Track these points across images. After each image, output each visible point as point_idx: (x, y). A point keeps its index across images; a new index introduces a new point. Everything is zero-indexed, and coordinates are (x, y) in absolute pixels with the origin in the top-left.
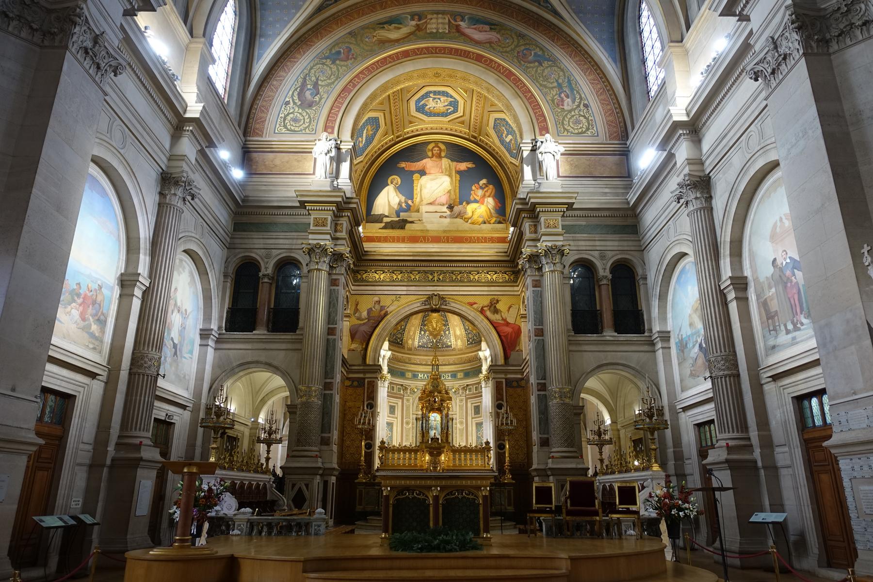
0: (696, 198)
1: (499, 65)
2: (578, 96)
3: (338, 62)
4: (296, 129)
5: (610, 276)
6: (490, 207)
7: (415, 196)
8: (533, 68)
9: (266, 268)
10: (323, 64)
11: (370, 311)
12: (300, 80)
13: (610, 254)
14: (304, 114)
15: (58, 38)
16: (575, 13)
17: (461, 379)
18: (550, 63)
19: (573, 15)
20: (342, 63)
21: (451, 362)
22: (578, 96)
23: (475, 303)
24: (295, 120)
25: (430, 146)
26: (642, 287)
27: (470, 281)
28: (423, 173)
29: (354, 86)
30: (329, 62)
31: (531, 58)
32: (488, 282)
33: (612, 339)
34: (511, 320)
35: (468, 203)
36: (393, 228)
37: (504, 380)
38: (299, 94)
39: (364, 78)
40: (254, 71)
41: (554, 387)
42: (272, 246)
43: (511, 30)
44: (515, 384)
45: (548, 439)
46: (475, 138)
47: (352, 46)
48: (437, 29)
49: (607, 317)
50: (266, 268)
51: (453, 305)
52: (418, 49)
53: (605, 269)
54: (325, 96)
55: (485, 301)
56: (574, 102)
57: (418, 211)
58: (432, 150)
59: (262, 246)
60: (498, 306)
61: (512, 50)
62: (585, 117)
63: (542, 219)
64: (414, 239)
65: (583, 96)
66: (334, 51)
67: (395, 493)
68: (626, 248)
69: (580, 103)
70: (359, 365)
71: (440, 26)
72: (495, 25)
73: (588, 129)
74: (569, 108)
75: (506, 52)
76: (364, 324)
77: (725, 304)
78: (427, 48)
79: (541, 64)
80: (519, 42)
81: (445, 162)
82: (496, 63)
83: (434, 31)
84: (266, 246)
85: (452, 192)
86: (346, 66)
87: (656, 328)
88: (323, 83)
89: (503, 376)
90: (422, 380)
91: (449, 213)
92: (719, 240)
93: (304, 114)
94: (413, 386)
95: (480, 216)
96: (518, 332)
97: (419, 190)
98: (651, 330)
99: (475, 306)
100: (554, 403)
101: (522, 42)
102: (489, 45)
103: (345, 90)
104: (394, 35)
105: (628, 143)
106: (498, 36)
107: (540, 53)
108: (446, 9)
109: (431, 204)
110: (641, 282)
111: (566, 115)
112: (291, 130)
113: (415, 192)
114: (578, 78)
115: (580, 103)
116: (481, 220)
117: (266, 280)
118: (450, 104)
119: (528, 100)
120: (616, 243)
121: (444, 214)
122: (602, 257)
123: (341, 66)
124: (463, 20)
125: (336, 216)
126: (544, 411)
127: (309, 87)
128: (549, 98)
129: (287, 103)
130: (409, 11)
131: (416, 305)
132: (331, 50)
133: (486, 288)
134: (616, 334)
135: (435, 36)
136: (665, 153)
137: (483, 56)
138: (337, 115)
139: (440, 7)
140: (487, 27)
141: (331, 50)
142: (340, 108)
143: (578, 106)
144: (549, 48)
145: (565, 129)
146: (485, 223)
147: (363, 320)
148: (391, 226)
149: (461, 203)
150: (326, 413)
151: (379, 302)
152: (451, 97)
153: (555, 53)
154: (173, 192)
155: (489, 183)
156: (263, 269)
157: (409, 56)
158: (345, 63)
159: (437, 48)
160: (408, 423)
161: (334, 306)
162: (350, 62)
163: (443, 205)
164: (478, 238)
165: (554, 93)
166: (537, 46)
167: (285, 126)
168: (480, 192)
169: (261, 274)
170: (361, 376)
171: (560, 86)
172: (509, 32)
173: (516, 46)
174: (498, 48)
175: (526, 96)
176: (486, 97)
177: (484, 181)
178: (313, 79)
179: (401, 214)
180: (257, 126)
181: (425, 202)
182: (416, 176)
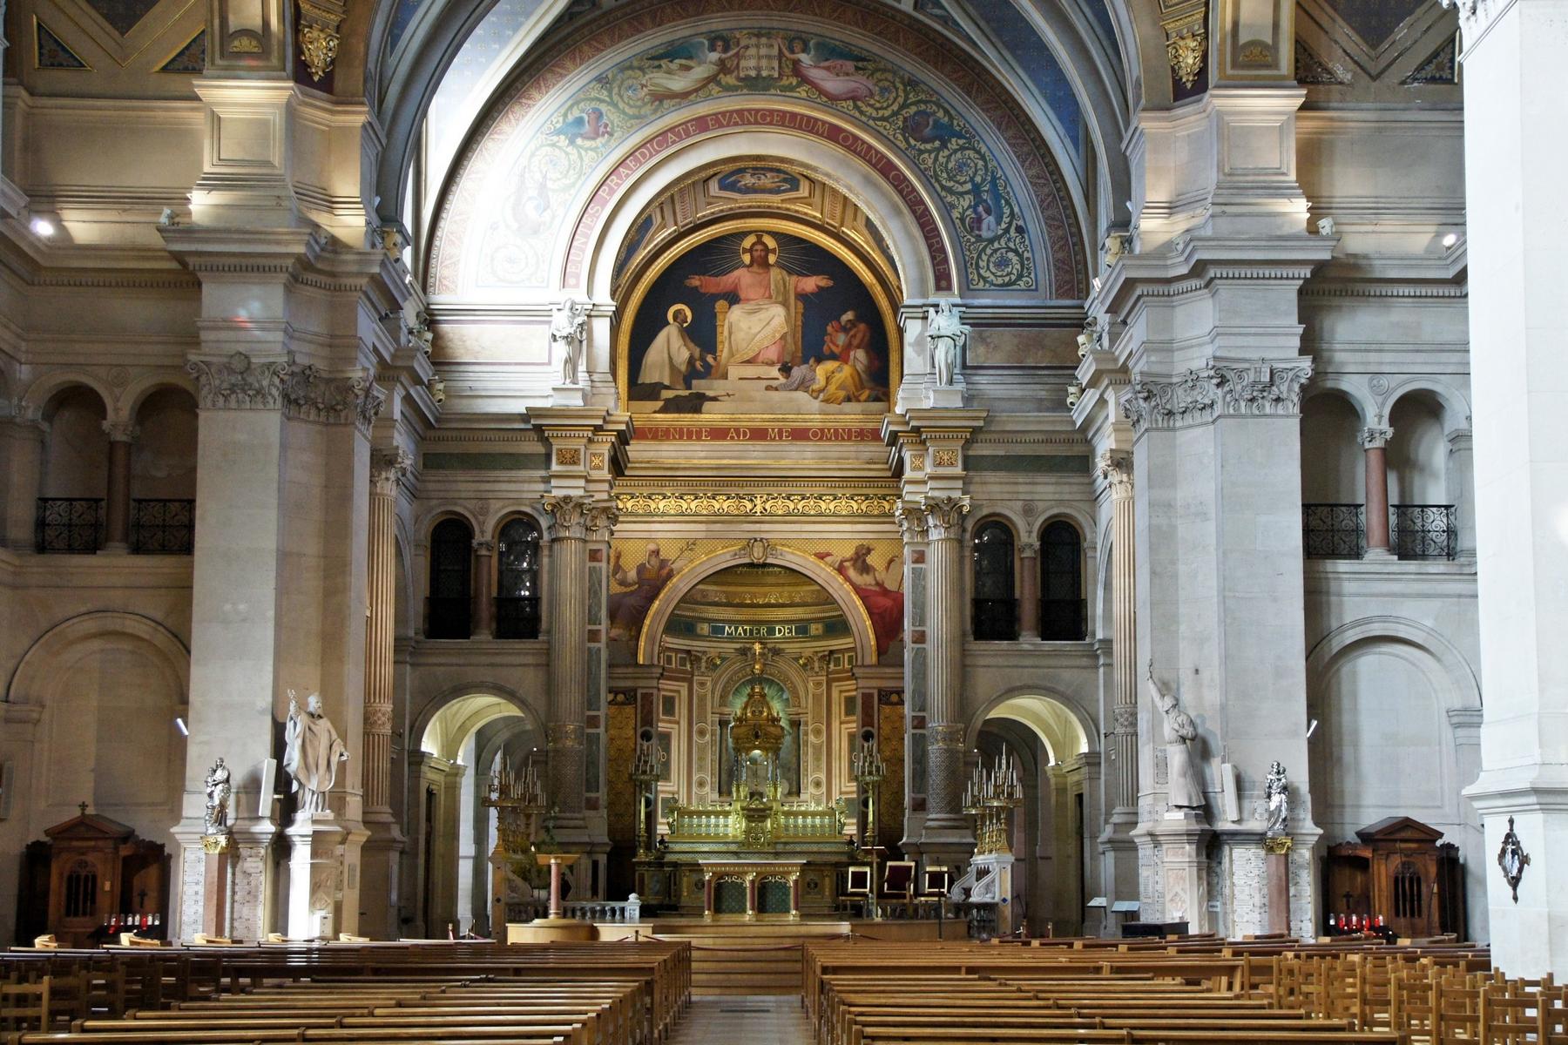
1: (870, 147)
2: (1007, 211)
3: (579, 141)
5: (1037, 544)
6: (860, 367)
7: (719, 347)
8: (930, 152)
9: (482, 532)
10: (553, 145)
11: (641, 569)
15: (343, 414)
16: (1007, 47)
17: (817, 638)
18: (961, 142)
19: (1005, 52)
20: (588, 143)
22: (1007, 211)
23: (828, 554)
25: (748, 242)
26: (1089, 561)
28: (733, 298)
30: (563, 141)
31: (927, 131)
32: (852, 515)
34: (891, 585)
35: (819, 361)
36: (679, 410)
41: (937, 724)
44: (894, 698)
45: (924, 800)
47: (603, 108)
48: (758, 69)
49: (1028, 610)
51: (789, 557)
53: (1030, 532)
55: (849, 552)
56: (999, 223)
57: (725, 376)
58: (751, 250)
59: (472, 495)
60: (869, 560)
61: (895, 114)
62: (1016, 251)
63: (931, 450)
64: (719, 434)
65: (1016, 209)
66: (570, 118)
69: (1010, 224)
70: (626, 666)
71: (764, 63)
72: (863, 59)
73: (1020, 277)
75: (883, 119)
76: (632, 593)
78: (740, 112)
79: (944, 146)
80: (907, 98)
81: (776, 274)
82: (864, 142)
83: (753, 73)
84: (479, 495)
86: (594, 149)
87: (1100, 635)
89: (875, 683)
90: (731, 638)
91: (782, 380)
94: (713, 653)
95: (841, 387)
97: (726, 333)
98: (1094, 635)
99: (828, 559)
100: (935, 750)
104: (678, 83)
108: (775, 24)
109: (749, 362)
110: (1089, 554)
111: (984, 249)
113: (719, 338)
114: (1009, 173)
115: (1010, 224)
116: (842, 394)
120: (1051, 489)
121: (774, 383)
122: (1028, 511)
123: (586, 150)
124: (805, 50)
125: (590, 440)
126: (920, 759)
128: (956, 214)
130: (704, 29)
132: (565, 115)
134: (1038, 641)
135: (755, 84)
139: (760, 20)
140: (849, 65)
141: (565, 115)
143: (1007, 231)
145: (980, 275)
146: (849, 399)
147: (630, 585)
148: (672, 406)
149: (806, 361)
150: (592, 763)
151: (657, 553)
154: (384, 475)
155: (859, 318)
159: (757, 111)
160: (702, 733)
161: (596, 593)
162: (600, 141)
163: (772, 364)
164: (836, 431)
166: (939, 106)
168: (841, 339)
169: (475, 543)
170: (629, 684)
171: (976, 190)
172: (890, 76)
174: (870, 110)
176: (845, 198)
177: (849, 316)
178: (538, 176)
182: (720, 305)
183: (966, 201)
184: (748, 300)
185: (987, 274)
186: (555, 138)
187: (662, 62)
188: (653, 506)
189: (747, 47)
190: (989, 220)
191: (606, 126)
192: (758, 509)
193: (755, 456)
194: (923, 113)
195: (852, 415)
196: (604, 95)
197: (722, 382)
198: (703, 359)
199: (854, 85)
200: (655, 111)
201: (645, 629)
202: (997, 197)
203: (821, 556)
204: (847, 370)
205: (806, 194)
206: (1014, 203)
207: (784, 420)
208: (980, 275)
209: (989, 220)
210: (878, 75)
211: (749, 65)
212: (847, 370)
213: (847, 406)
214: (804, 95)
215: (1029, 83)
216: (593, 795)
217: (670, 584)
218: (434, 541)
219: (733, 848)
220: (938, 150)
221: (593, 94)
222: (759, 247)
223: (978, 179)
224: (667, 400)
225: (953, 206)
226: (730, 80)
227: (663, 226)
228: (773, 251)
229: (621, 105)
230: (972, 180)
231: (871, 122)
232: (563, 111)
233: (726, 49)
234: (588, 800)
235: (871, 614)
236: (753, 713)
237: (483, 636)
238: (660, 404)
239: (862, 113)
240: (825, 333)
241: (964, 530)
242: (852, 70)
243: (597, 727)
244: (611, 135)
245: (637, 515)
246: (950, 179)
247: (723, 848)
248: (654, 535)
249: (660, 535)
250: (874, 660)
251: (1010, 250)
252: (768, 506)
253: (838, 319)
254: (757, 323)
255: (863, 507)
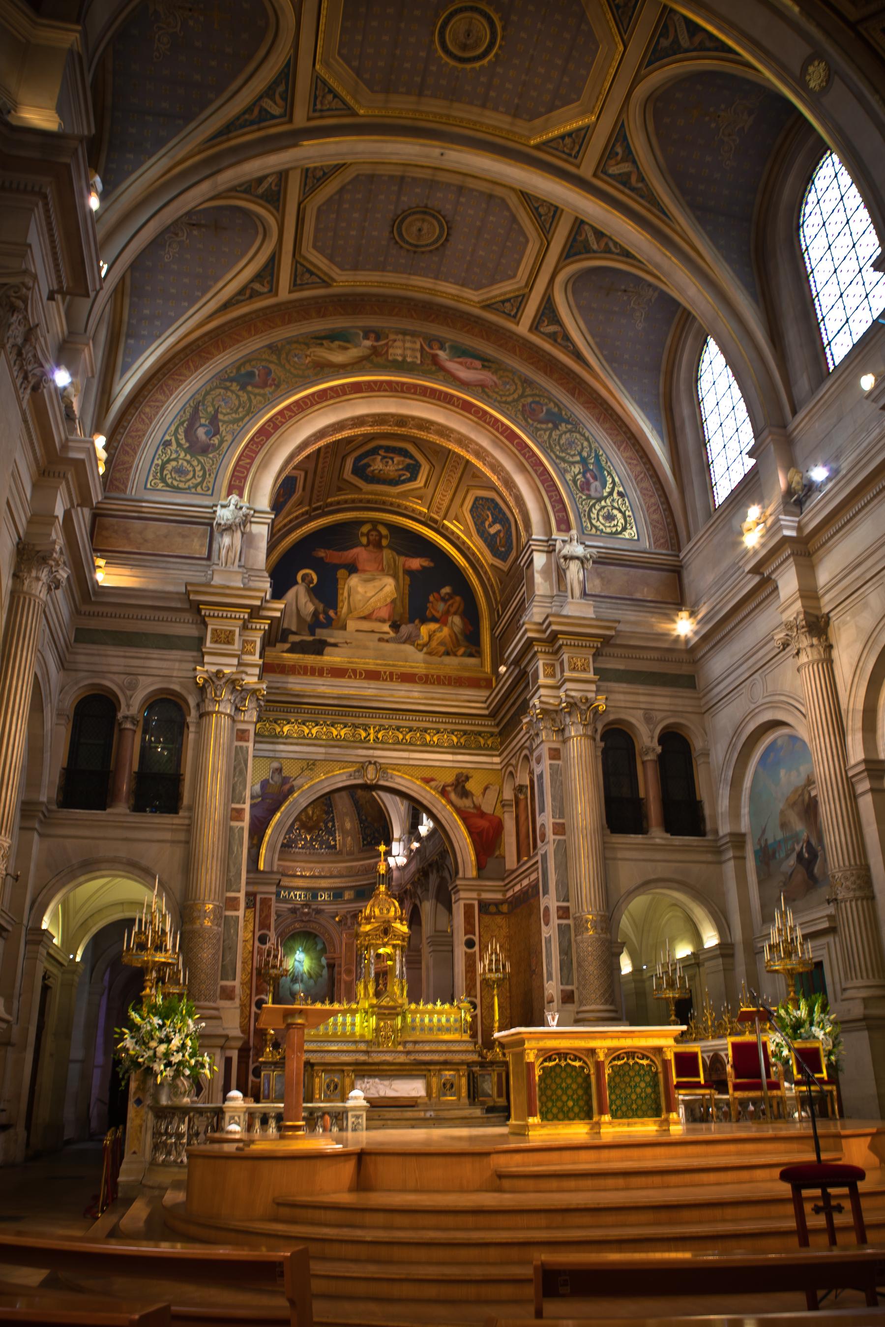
0: (812, 646)
2: (609, 480)
3: (249, 388)
4: (181, 485)
5: (659, 749)
6: (456, 629)
7: (340, 605)
8: (545, 430)
9: (128, 706)
10: (227, 389)
12: (189, 410)
13: (660, 715)
14: (195, 463)
16: (607, 360)
18: (569, 426)
20: (257, 391)
21: (335, 873)
22: (609, 480)
23: (432, 780)
24: (180, 471)
25: (365, 529)
27: (426, 745)
28: (352, 569)
29: (276, 428)
30: (235, 387)
31: (542, 415)
33: (663, 842)
34: (487, 808)
35: (424, 620)
36: (304, 652)
37: (476, 903)
38: (186, 432)
39: (291, 417)
40: (117, 388)
42: (140, 671)
43: (514, 372)
44: (493, 909)
46: (436, 522)
47: (272, 367)
48: (404, 357)
50: (128, 706)
51: (399, 780)
52: (375, 382)
53: (652, 738)
54: (229, 438)
55: (450, 778)
57: (344, 628)
58: (367, 535)
60: (470, 786)
61: (514, 401)
62: (620, 511)
63: (565, 657)
64: (338, 672)
65: (617, 479)
66: (243, 371)
67: (541, 1059)
68: (680, 709)
69: (613, 489)
71: (409, 352)
73: (624, 529)
74: (598, 495)
75: (506, 402)
77: (854, 797)
78: (389, 383)
79: (556, 427)
80: (523, 392)
81: (387, 554)
82: (492, 416)
83: (400, 358)
84: (128, 670)
85: (398, 603)
86: (263, 395)
87: (724, 829)
88: (226, 418)
89: (474, 895)
91: (392, 634)
92: (843, 706)
93: (195, 463)
95: (442, 643)
96: (498, 827)
97: (346, 594)
98: (716, 832)
99: (433, 784)
101: (528, 391)
102: (481, 389)
103: (264, 433)
104: (338, 358)
105: (682, 555)
106: (495, 378)
107: (556, 410)
108: (418, 329)
112: (172, 486)
113: (340, 598)
115: (613, 489)
116: (442, 649)
117: (128, 725)
118: (407, 468)
119: (539, 476)
120: (667, 700)
121: (386, 637)
122: (648, 719)
123: (255, 395)
124: (442, 348)
127: (203, 421)
128: (569, 477)
129: (167, 444)
130: (360, 324)
131: (339, 779)
133: (450, 757)
134: (668, 836)
135: (400, 366)
136: (757, 579)
137: (473, 405)
138: (248, 470)
140: (478, 364)
141: (238, 369)
142: (253, 459)
143: (611, 494)
144: (568, 405)
145: (592, 524)
146: (447, 653)
149: (411, 621)
151: (279, 770)
152: (412, 457)
153: (577, 413)
154: (34, 574)
155: (455, 592)
156: (123, 706)
157: (360, 391)
158: (262, 391)
162: (268, 390)
163: (383, 621)
164: (438, 677)
165: (577, 471)
166: (550, 400)
167: (163, 479)
168: (441, 606)
169: (120, 716)
171: (584, 461)
173: (522, 396)
174: (495, 396)
175: (536, 471)
177: (446, 590)
178: (210, 409)
179: (318, 631)
180: (118, 475)
181: (356, 614)
182: (341, 573)
183: (576, 469)
184: (364, 571)
185: (598, 524)
186: (228, 384)
187: (325, 342)
188: (278, 729)
189: (395, 341)
190: (595, 484)
191: (274, 380)
192: (372, 737)
193: (368, 690)
194: (538, 403)
195: (452, 664)
196: (274, 358)
197: (341, 632)
198: (326, 613)
199: (482, 377)
200: (316, 374)
201: (266, 839)
202: (601, 469)
203: (427, 781)
204: (446, 631)
205: (422, 484)
206: (614, 475)
207: (394, 666)
208: (592, 524)
209: (595, 484)
210: (501, 373)
211: (396, 352)
212: (446, 631)
213: (447, 660)
214: (441, 378)
215: (623, 388)
216: (229, 983)
217: (291, 799)
218: (76, 714)
219: (363, 1047)
220: (552, 430)
221: (264, 356)
222: (374, 533)
223: (585, 454)
224: (293, 644)
225: (566, 471)
226: (380, 360)
227: (300, 503)
228: (386, 537)
229: (288, 367)
230: (580, 454)
231: (497, 404)
232: (238, 364)
233: (377, 339)
234: (223, 989)
235: (471, 833)
236: (381, 910)
237: (121, 809)
238: (287, 646)
239: (488, 396)
240: (428, 601)
241: (596, 731)
242: (480, 366)
243: (237, 910)
244: (278, 386)
245: (264, 736)
246: (563, 451)
247: (352, 1047)
248: (278, 755)
249: (283, 755)
250: (472, 872)
251: (613, 508)
252: (380, 735)
253: (438, 592)
254: (371, 590)
255: (462, 740)
